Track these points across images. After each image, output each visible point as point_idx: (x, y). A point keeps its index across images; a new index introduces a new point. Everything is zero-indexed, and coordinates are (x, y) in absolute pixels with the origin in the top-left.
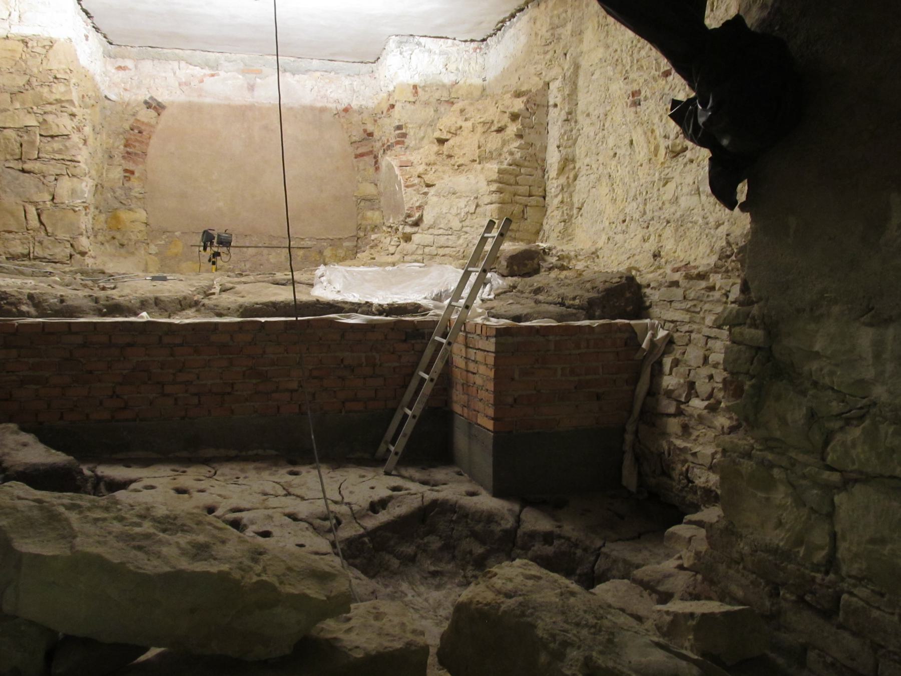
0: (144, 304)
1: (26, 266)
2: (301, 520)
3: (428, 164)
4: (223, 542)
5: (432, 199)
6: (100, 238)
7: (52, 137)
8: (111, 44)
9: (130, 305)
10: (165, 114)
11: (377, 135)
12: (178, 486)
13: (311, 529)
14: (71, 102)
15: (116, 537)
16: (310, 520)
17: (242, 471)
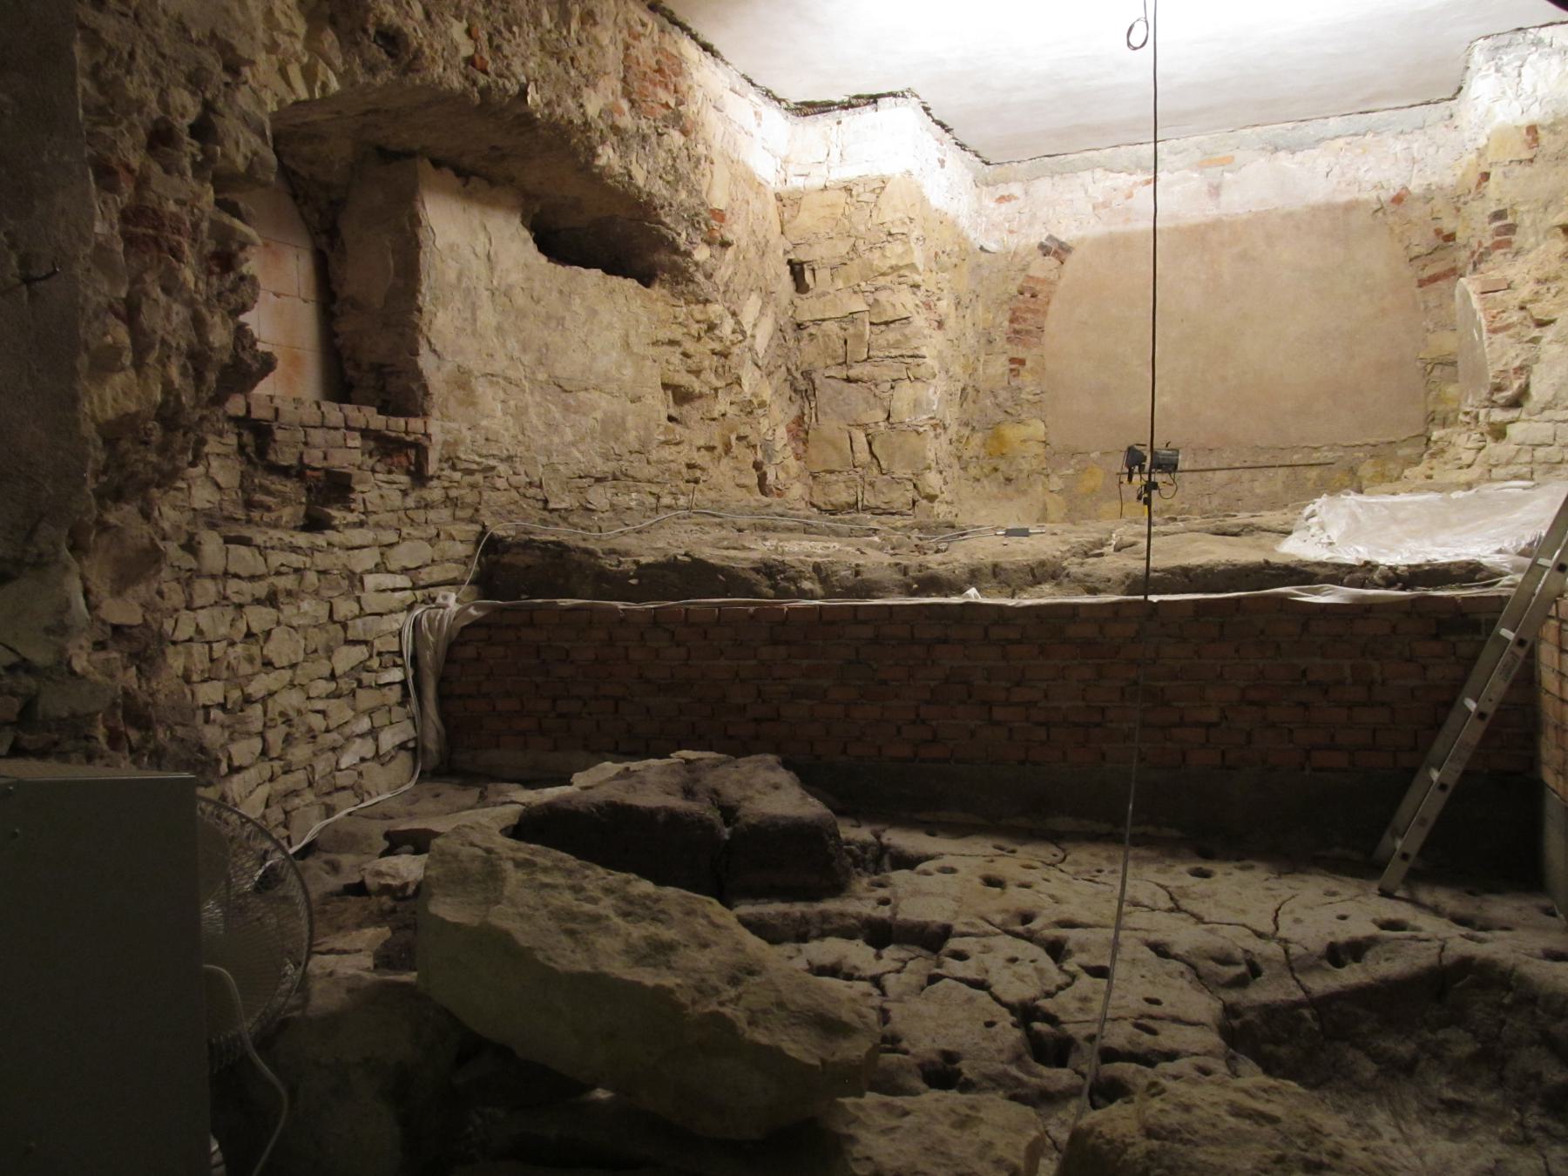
0: (974, 576)
1: (843, 521)
2: (1176, 957)
3: (1538, 281)
4: (705, 945)
5: (1550, 348)
6: (973, 471)
7: (886, 323)
8: (988, 164)
9: (952, 577)
10: (1071, 260)
11: (1461, 237)
12: (992, 873)
13: (1189, 976)
14: (912, 267)
15: (551, 912)
16: (1193, 960)
17: (1110, 859)
